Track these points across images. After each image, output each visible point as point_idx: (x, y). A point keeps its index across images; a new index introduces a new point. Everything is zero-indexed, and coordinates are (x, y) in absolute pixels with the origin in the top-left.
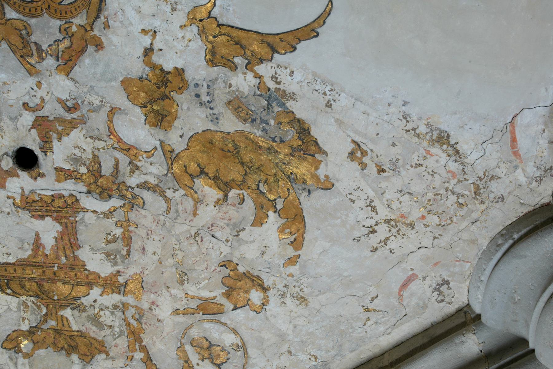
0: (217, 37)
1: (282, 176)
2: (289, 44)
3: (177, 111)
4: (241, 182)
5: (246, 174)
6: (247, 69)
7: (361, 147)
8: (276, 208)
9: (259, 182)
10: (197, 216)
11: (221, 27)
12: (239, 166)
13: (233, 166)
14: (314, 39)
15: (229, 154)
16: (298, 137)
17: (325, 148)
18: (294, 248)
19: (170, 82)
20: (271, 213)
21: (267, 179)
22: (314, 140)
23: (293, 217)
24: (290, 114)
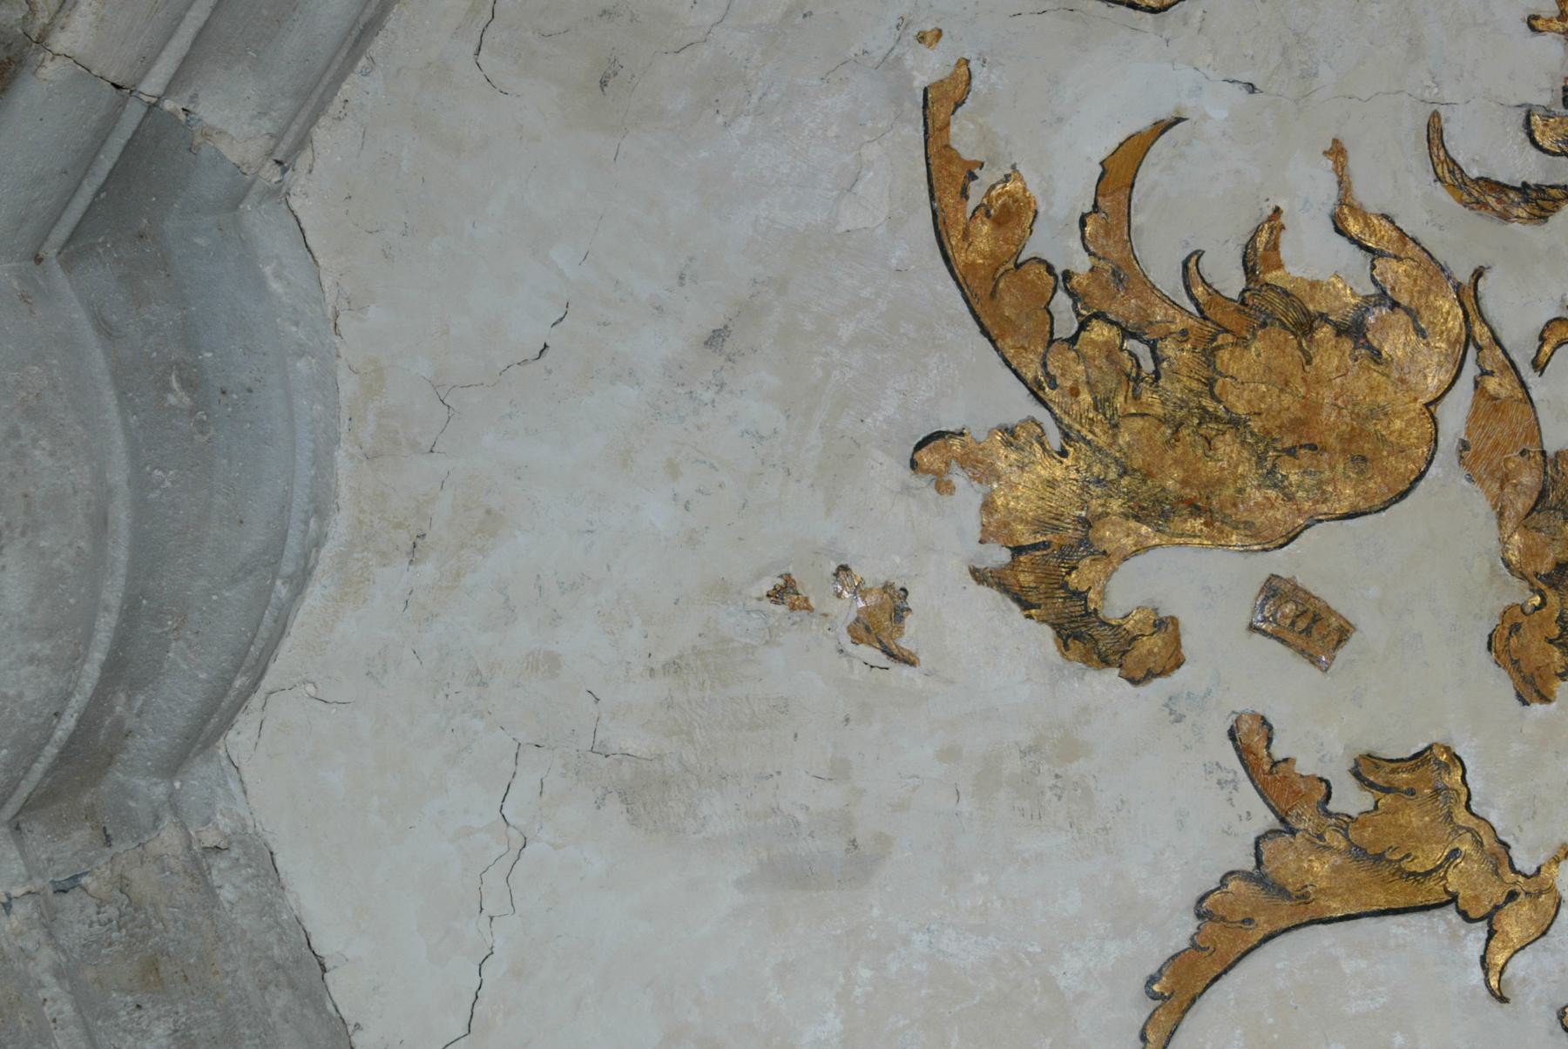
0: (1447, 859)
1: (1091, 432)
2: (1223, 919)
3: (1504, 542)
4: (1219, 348)
5: (1210, 383)
6: (1321, 780)
7: (878, 653)
8: (1071, 293)
9: (1157, 375)
10: (1329, 145)
11: (1446, 898)
12: (1241, 409)
13: (1263, 398)
14: (1152, 969)
15: (1288, 443)
16: (1086, 599)
17: (989, 596)
18: (959, 157)
19: (1551, 642)
20: (1081, 264)
21: (1136, 397)
22: (1033, 611)
23: (1001, 285)
24: (1139, 674)
